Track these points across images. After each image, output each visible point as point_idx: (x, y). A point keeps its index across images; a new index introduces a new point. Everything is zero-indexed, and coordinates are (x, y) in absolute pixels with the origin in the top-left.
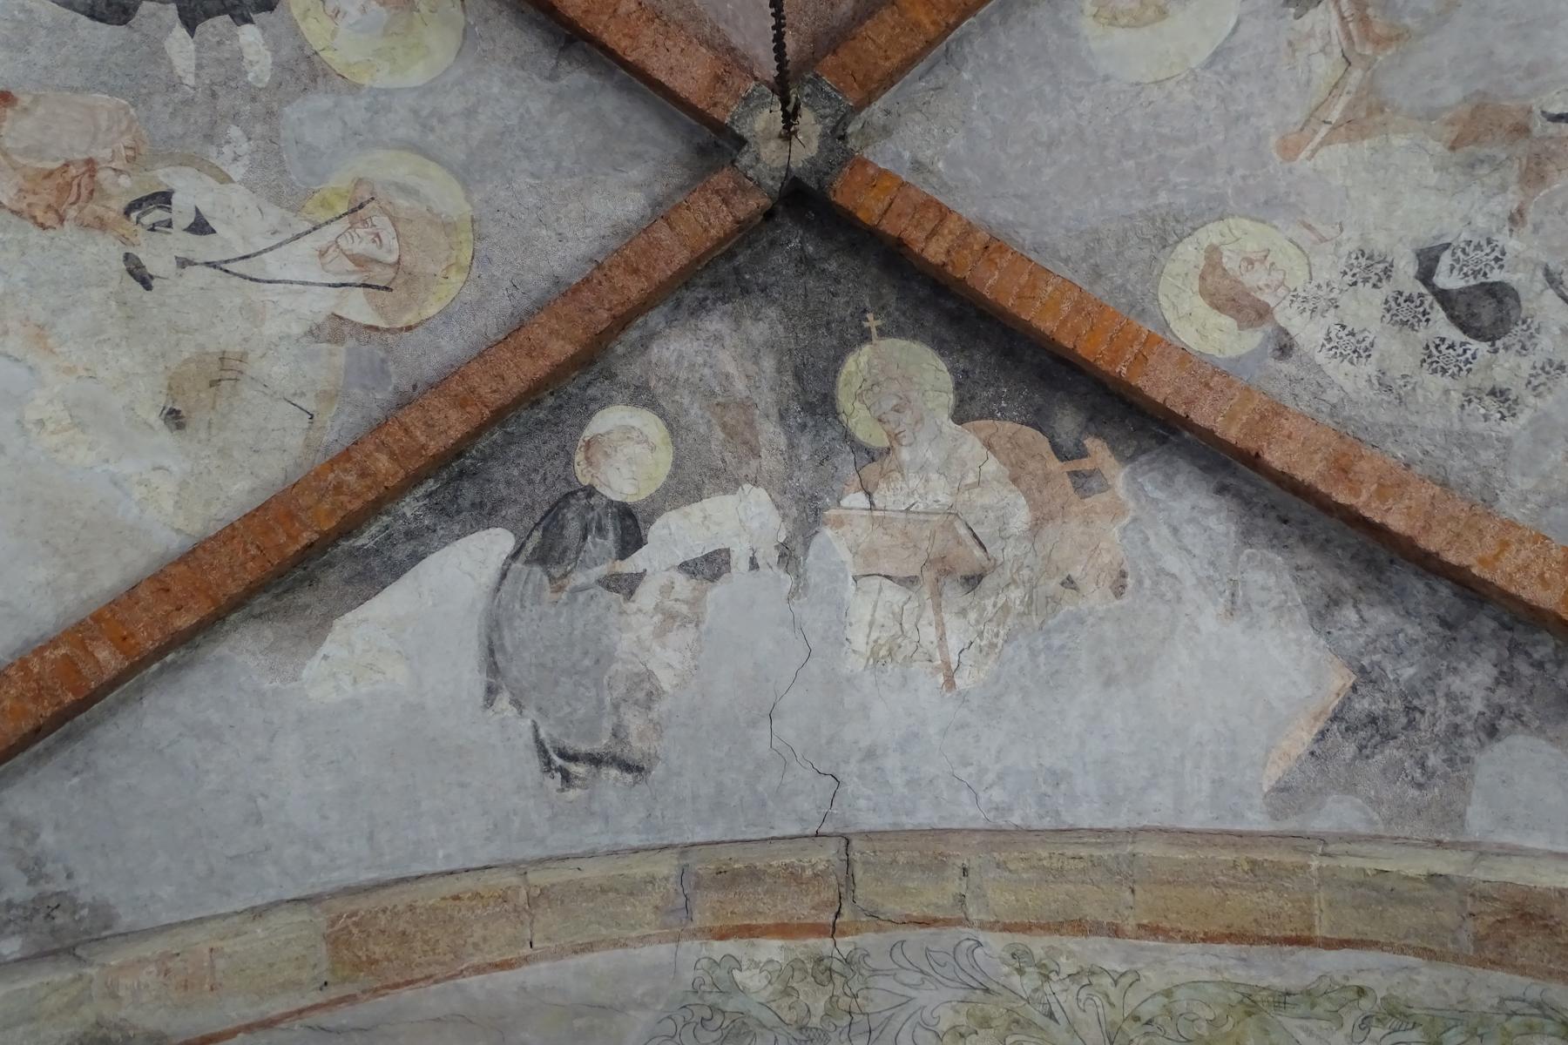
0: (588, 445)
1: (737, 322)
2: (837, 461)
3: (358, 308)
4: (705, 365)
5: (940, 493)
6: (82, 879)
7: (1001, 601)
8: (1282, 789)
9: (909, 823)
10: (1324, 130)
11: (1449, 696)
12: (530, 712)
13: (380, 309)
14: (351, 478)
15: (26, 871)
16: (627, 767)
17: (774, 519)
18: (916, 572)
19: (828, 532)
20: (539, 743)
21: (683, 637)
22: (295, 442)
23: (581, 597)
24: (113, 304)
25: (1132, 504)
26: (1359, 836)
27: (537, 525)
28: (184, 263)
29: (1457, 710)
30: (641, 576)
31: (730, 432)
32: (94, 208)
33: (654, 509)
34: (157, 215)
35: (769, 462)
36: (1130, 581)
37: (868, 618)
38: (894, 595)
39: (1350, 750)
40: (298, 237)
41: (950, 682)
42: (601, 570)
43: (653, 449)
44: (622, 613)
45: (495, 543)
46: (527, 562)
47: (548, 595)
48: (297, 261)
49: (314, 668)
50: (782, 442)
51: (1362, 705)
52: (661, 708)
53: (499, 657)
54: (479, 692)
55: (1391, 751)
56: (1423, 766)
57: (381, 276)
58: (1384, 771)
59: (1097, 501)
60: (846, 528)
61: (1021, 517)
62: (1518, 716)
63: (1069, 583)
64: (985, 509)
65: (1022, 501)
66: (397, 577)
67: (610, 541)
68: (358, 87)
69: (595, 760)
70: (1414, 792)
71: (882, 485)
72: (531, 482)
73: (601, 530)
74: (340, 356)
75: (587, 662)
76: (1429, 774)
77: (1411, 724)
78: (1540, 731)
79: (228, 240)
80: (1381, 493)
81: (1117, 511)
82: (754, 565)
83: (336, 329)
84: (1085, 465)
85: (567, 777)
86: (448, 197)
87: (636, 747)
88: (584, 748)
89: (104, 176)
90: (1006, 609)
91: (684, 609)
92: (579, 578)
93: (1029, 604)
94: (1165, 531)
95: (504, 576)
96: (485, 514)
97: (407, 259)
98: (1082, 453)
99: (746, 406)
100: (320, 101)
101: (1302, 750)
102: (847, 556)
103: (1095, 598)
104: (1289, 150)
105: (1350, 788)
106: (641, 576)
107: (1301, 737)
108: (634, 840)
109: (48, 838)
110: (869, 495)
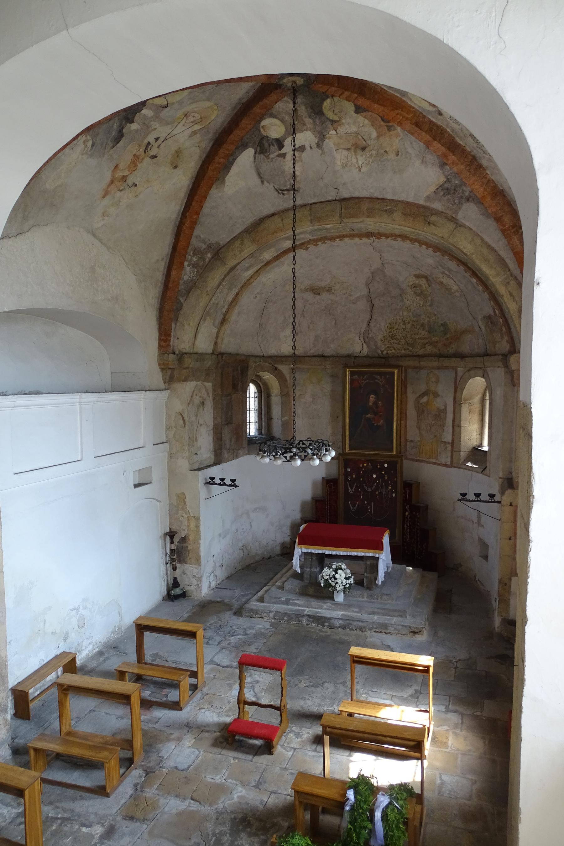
0: (263, 127)
2: (327, 124)
3: (197, 127)
4: (286, 108)
5: (354, 129)
7: (370, 154)
8: (428, 197)
9: (354, 195)
11: (463, 190)
14: (217, 165)
15: (203, 243)
17: (313, 137)
18: (349, 147)
19: (327, 140)
20: (276, 189)
22: (197, 150)
23: (274, 160)
24: (154, 165)
25: (401, 134)
26: (439, 211)
27: (258, 146)
28: (159, 147)
29: (463, 193)
32: (141, 158)
34: (150, 147)
35: (309, 126)
36: (400, 153)
37: (340, 158)
38: (345, 153)
39: (442, 193)
40: (177, 126)
41: (360, 170)
42: (276, 154)
43: (279, 127)
44: (284, 162)
45: (249, 153)
46: (259, 154)
47: (266, 160)
48: (180, 128)
49: (226, 189)
50: (311, 121)
51: (446, 186)
53: (261, 175)
54: (260, 182)
55: (449, 197)
56: (454, 201)
57: (197, 121)
58: (447, 200)
59: (393, 132)
60: (331, 139)
61: (374, 135)
62: (473, 199)
63: (386, 152)
64: (365, 132)
65: (375, 131)
66: (232, 165)
67: (276, 146)
68: (174, 103)
70: (451, 206)
71: (339, 127)
72: (252, 137)
73: (273, 145)
74: (198, 135)
75: (280, 173)
77: (454, 193)
78: (476, 204)
81: (397, 135)
82: (311, 148)
85: (283, 194)
88: (285, 188)
90: (371, 155)
92: (272, 156)
93: (377, 154)
94: (409, 143)
95: (255, 158)
96: (245, 146)
97: (203, 116)
102: (332, 146)
103: (392, 156)
107: (433, 188)
109: (202, 236)
110: (336, 131)
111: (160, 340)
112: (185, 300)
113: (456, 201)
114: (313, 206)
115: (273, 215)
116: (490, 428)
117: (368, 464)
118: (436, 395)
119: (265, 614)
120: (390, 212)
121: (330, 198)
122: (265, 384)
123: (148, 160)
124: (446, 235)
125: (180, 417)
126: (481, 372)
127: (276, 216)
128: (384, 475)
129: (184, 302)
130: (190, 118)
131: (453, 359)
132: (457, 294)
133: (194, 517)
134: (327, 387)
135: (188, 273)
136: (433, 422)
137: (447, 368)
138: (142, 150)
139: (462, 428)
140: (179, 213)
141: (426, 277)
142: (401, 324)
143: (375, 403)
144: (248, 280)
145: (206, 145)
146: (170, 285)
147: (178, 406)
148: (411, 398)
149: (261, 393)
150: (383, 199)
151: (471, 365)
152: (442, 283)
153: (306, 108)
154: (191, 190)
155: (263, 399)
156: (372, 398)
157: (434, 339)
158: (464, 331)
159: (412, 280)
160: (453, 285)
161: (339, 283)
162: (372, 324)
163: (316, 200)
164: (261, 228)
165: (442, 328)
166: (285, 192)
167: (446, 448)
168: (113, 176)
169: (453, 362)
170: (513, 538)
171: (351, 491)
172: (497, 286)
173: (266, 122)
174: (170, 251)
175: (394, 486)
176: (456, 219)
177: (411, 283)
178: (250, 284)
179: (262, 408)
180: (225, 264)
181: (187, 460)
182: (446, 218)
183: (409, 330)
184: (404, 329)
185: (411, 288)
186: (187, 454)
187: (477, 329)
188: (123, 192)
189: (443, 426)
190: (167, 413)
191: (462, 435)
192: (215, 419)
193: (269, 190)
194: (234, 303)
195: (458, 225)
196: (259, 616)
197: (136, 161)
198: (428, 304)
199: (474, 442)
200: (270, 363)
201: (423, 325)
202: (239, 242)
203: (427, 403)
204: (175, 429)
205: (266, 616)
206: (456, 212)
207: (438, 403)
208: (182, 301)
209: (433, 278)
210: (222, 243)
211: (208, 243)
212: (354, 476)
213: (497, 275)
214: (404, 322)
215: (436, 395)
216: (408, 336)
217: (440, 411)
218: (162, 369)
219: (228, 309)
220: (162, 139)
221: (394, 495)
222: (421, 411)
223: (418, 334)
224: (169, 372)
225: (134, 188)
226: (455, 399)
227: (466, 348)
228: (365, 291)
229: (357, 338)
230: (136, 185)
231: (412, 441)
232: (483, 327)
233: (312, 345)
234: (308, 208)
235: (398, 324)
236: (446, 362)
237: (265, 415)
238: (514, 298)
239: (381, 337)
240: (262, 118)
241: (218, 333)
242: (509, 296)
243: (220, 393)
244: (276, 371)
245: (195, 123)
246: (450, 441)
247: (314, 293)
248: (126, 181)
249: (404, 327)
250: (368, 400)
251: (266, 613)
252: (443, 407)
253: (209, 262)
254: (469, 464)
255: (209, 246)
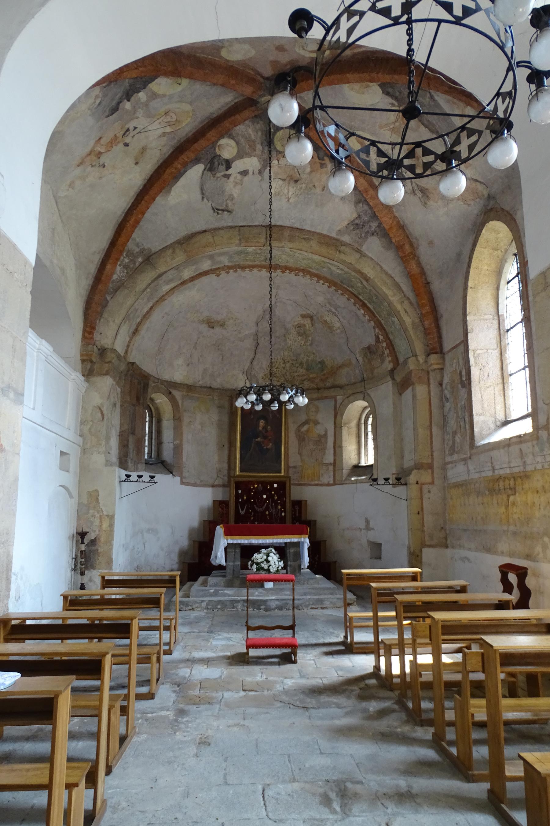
0: (219, 146)
1: (253, 124)
3: (168, 130)
6: (145, 245)
8: (339, 231)
10: (388, 128)
11: (370, 226)
12: (210, 202)
13: (172, 128)
14: (174, 170)
16: (228, 211)
18: (285, 178)
20: (212, 207)
21: (239, 187)
23: (219, 179)
28: (133, 137)
29: (370, 228)
30: (230, 175)
31: (250, 146)
33: (233, 160)
34: (128, 133)
36: (325, 189)
38: (280, 182)
39: (352, 228)
41: (288, 201)
42: (222, 173)
43: (233, 148)
45: (199, 168)
47: (212, 178)
48: (156, 125)
49: (170, 198)
50: (261, 148)
51: (357, 221)
52: (234, 201)
54: (201, 199)
55: (357, 231)
56: (361, 235)
57: (172, 123)
62: (377, 234)
63: (314, 186)
66: (181, 176)
67: (224, 167)
69: (223, 210)
73: (222, 165)
74: (165, 138)
76: (361, 237)
77: (362, 228)
78: (379, 238)
79: (140, 127)
80: (371, 198)
82: (253, 173)
83: (164, 134)
84: (323, 162)
85: (218, 213)
86: (187, 107)
87: (230, 207)
88: (221, 208)
89: (117, 135)
90: (301, 188)
91: (239, 182)
92: (218, 175)
95: (203, 174)
96: (197, 161)
97: (178, 119)
98: (323, 160)
99: (254, 141)
100: (158, 100)
101: (345, 225)
103: (318, 190)
104: (381, 127)
105: (349, 235)
106: (230, 175)
107: (346, 223)
108: (230, 224)
109: (138, 240)
110: (278, 161)
111: (84, 331)
112: (112, 298)
113: (363, 235)
114: (242, 228)
115: (205, 231)
116: (375, 439)
117: (258, 486)
118: (316, 423)
119: (197, 605)
120: (308, 240)
121: (257, 224)
122: (157, 409)
123: (121, 145)
124: (353, 262)
125: (98, 410)
126: (361, 395)
127: (208, 232)
128: (274, 495)
129: (110, 300)
130: (168, 117)
131: (333, 389)
132: (338, 331)
133: (108, 516)
134: (214, 416)
135: (119, 272)
136: (315, 447)
137: (326, 398)
138: (122, 133)
139: (344, 449)
140: (124, 210)
141: (311, 317)
142: (281, 364)
143: (265, 428)
144: (163, 296)
145: (167, 151)
146: (103, 279)
147: (97, 399)
148: (292, 428)
149: (152, 417)
150: (302, 230)
151: (350, 392)
152: (326, 321)
153: (262, 134)
154: (141, 191)
155: (154, 423)
156: (262, 423)
157: (311, 376)
158: (340, 367)
159: (299, 320)
160: (336, 322)
161: (232, 318)
162: (255, 363)
163: (244, 224)
164: (193, 241)
165: (319, 366)
166: (220, 212)
167: (328, 469)
168: (94, 147)
169: (332, 393)
170: (421, 513)
171: (242, 512)
172: (395, 304)
173: (224, 141)
174: (107, 247)
175: (284, 505)
176: (361, 251)
177: (296, 323)
178: (164, 300)
179: (152, 432)
180: (156, 269)
181: (103, 455)
182: (353, 249)
183: (288, 369)
184: (284, 368)
185: (295, 328)
186: (104, 449)
187: (354, 361)
188: (93, 168)
189: (324, 449)
190: (83, 407)
191: (344, 455)
192: (121, 425)
193: (206, 206)
194: (147, 316)
195: (363, 255)
196: (190, 608)
197: (114, 141)
198: (308, 344)
199: (354, 462)
200: (165, 387)
201: (301, 364)
202: (171, 251)
203: (308, 431)
204: (91, 423)
205: (197, 607)
206: (361, 245)
207: (319, 430)
208: (108, 298)
209: (318, 318)
210: (154, 250)
211: (141, 248)
212: (245, 498)
213: (395, 295)
214: (284, 361)
215: (316, 423)
216: (288, 374)
217: (320, 436)
218: (83, 361)
219: (142, 321)
220: (137, 130)
221: (283, 514)
222: (302, 439)
223: (296, 372)
224: (89, 365)
225: (101, 168)
226: (335, 423)
227: (342, 380)
228: (253, 330)
229: (241, 375)
230: (104, 166)
231: (295, 467)
232: (360, 359)
233: (201, 377)
234: (237, 229)
235: (278, 363)
236: (326, 393)
237: (155, 439)
238: (408, 313)
239: (262, 375)
240: (222, 137)
241: (129, 342)
242: (404, 312)
243: (129, 400)
244: (170, 396)
245: (170, 124)
246: (332, 461)
247: (209, 326)
248: (99, 158)
249: (284, 366)
250: (258, 425)
251: (197, 603)
252: (323, 433)
253: (140, 265)
254: (353, 479)
255: (141, 251)
